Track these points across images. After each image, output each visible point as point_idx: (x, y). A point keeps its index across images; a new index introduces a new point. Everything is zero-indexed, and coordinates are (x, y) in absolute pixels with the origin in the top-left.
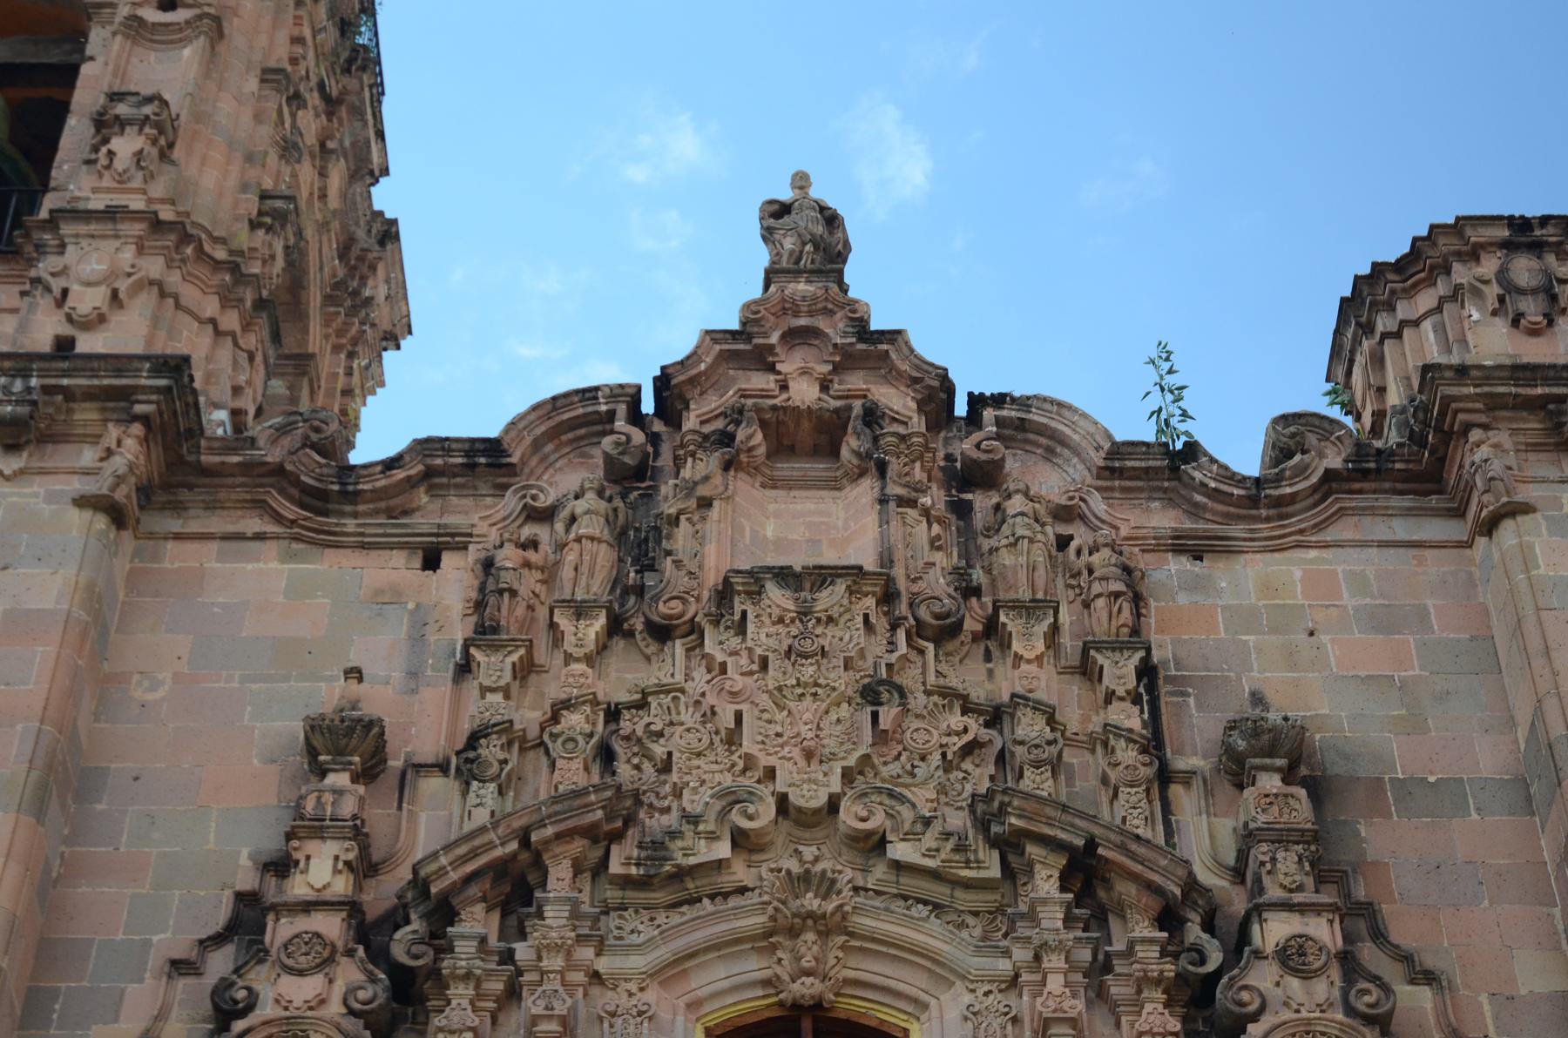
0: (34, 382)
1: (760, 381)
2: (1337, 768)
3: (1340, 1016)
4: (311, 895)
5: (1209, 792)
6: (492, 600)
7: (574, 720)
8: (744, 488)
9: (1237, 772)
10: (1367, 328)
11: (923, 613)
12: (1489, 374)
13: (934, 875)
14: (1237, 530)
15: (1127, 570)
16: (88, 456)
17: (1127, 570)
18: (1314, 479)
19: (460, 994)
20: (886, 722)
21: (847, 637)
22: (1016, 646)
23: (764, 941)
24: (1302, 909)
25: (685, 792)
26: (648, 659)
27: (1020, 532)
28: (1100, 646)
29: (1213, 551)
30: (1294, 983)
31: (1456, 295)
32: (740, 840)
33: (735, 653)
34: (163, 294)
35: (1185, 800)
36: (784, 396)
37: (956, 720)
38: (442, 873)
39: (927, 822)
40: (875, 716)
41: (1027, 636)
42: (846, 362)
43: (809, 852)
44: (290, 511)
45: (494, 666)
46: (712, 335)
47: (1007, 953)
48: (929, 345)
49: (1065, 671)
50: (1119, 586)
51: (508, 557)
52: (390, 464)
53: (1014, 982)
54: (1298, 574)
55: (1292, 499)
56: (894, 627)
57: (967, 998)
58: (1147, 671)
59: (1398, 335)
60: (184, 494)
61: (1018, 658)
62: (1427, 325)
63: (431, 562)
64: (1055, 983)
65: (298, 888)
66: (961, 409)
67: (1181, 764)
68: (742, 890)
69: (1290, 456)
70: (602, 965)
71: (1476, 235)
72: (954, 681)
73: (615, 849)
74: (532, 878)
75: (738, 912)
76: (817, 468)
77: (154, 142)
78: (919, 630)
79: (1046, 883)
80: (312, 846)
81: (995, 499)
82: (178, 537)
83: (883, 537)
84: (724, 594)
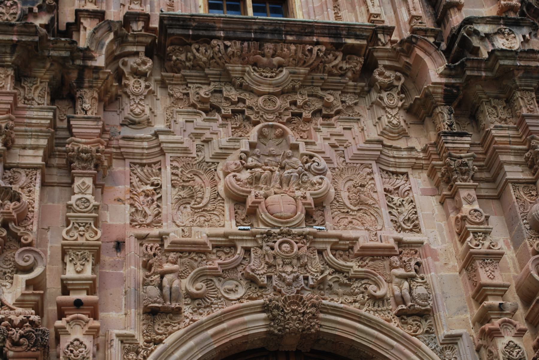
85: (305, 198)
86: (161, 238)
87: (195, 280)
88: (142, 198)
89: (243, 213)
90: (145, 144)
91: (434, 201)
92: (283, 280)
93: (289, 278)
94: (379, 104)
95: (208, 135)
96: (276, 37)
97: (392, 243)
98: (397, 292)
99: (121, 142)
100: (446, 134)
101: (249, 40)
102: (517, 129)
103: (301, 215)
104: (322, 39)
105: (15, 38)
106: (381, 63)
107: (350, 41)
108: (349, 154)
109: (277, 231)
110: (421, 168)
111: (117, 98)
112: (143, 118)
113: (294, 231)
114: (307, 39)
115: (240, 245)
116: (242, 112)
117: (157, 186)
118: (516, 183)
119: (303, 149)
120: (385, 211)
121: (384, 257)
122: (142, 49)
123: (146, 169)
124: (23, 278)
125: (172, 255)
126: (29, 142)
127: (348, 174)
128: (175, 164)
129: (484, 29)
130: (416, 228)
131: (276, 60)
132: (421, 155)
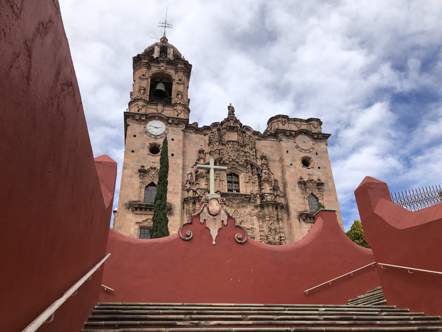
1: (228, 123)
2: (268, 158)
6: (211, 140)
7: (217, 151)
8: (227, 132)
10: (271, 121)
13: (241, 164)
15: (254, 141)
16: (181, 126)
20: (239, 153)
21: (236, 146)
23: (230, 168)
24: (266, 170)
28: (253, 148)
29: (260, 140)
32: (229, 161)
35: (258, 160)
37: (243, 153)
39: (242, 161)
42: (235, 122)
43: (233, 162)
44: (195, 131)
45: (211, 146)
46: (225, 119)
50: (254, 143)
51: (211, 136)
52: (202, 128)
53: (247, 173)
55: (266, 136)
56: (239, 145)
57: (244, 174)
58: (256, 150)
59: (274, 123)
60: (186, 128)
62: (276, 122)
63: (205, 136)
64: (250, 173)
66: (243, 126)
67: (258, 157)
69: (266, 133)
75: (229, 166)
76: (232, 130)
77: (182, 96)
79: (249, 166)
80: (201, 160)
81: (245, 135)
83: (238, 137)
84: (227, 142)
96: (237, 196)
97: (250, 228)
98: (250, 235)
100: (259, 212)
104: (244, 196)
108: (246, 213)
110: (256, 215)
114: (242, 196)
118: (267, 220)
119: (240, 213)
121: (249, 230)
127: (245, 217)
129: (266, 195)
131: (237, 199)
132: (256, 214)
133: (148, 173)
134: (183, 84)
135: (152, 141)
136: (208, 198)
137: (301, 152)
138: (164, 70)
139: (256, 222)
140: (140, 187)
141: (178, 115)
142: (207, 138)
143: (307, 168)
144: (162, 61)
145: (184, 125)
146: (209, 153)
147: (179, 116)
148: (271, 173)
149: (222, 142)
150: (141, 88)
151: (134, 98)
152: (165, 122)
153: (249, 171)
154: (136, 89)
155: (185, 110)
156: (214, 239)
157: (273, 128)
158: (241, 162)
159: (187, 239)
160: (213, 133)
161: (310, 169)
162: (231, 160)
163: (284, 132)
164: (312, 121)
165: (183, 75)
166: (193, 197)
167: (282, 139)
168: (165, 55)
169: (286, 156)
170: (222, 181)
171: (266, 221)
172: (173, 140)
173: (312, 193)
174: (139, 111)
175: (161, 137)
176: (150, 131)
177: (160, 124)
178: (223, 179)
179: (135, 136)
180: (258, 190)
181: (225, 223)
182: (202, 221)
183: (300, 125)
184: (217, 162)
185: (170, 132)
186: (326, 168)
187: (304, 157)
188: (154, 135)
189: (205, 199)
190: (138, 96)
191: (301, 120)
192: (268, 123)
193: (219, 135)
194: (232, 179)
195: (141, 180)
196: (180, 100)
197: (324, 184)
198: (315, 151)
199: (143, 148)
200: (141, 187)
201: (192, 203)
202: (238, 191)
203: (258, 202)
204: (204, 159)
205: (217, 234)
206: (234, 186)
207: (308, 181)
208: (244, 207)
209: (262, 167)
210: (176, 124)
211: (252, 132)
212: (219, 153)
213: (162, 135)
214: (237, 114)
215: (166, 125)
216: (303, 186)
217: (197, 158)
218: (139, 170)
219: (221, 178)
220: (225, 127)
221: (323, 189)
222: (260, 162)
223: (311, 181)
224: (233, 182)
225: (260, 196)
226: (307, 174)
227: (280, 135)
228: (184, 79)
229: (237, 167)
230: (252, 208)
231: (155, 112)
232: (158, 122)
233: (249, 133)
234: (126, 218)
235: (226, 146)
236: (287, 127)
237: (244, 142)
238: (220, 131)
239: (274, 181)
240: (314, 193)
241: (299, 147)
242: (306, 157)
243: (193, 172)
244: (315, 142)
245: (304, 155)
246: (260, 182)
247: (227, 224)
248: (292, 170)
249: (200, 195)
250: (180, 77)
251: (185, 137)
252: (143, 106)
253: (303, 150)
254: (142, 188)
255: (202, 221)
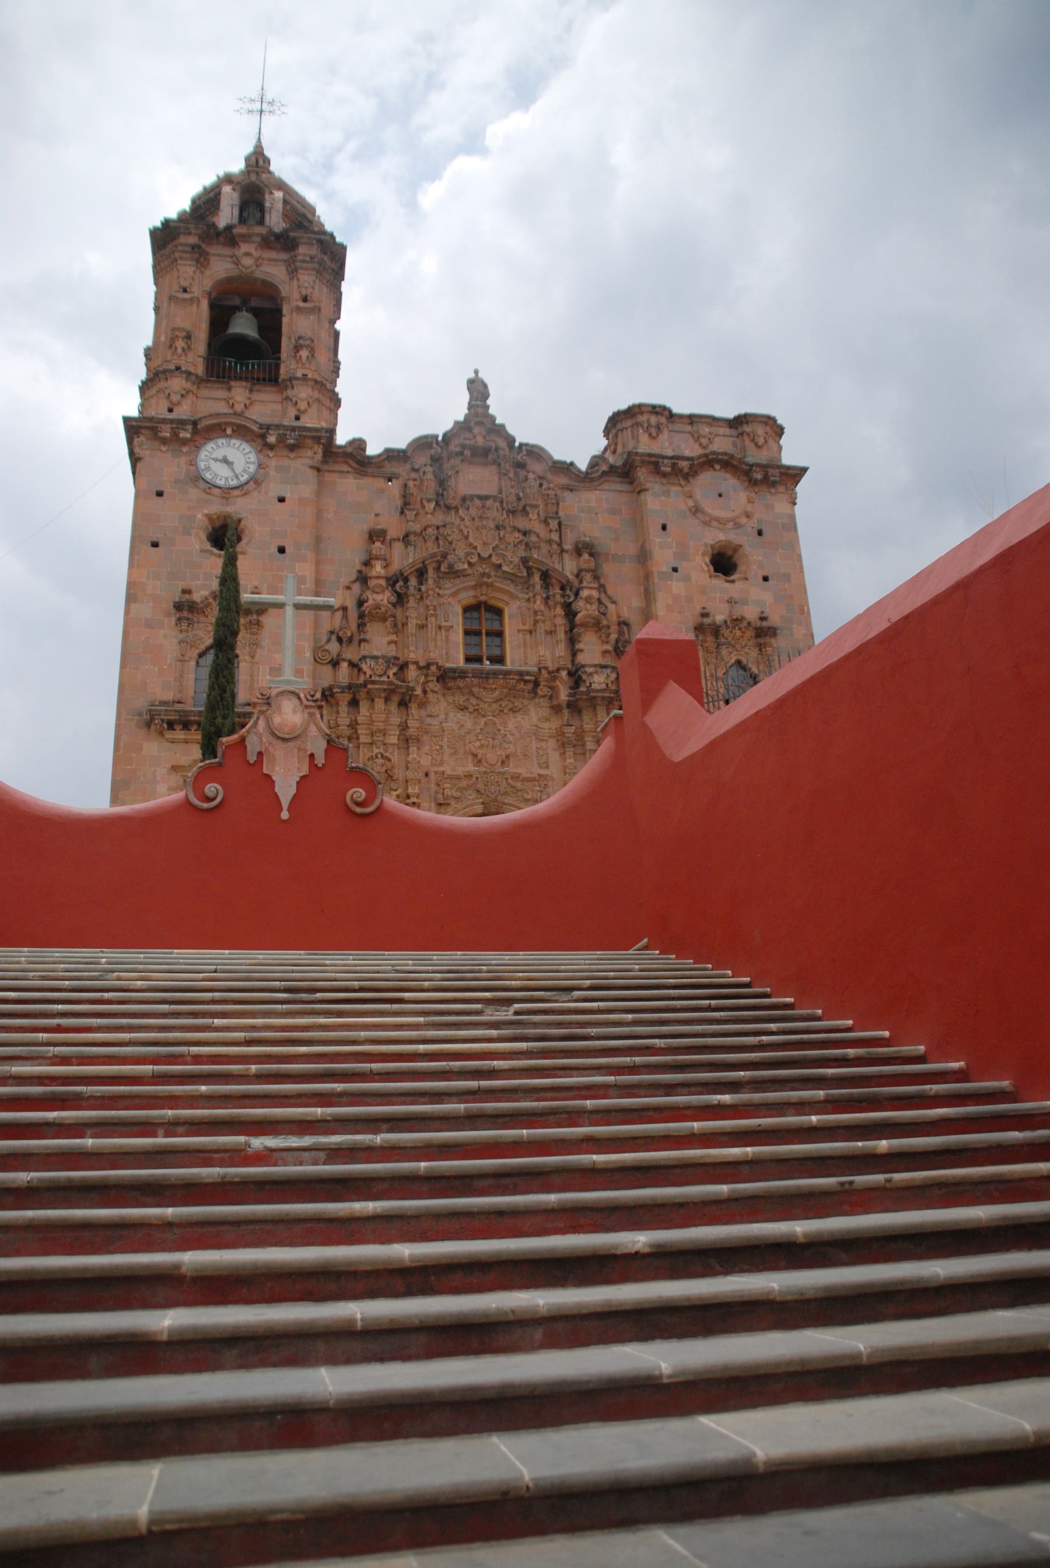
0: (296, 433)
1: (468, 435)
3: (597, 613)
4: (377, 575)
5: (571, 554)
7: (430, 530)
9: (578, 551)
10: (615, 426)
11: (509, 506)
12: (643, 455)
13: (513, 574)
14: (581, 485)
16: (309, 453)
17: (556, 495)
18: (600, 473)
19: (411, 599)
20: (501, 536)
21: (493, 514)
22: (531, 516)
23: (475, 587)
25: (456, 551)
26: (444, 513)
27: (532, 484)
29: (576, 490)
30: (588, 606)
31: (637, 424)
32: (470, 564)
33: (466, 515)
34: (319, 402)
35: (566, 556)
36: (474, 440)
37: (517, 535)
38: (407, 571)
40: (499, 534)
41: (533, 513)
43: (484, 566)
46: (456, 423)
47: (527, 593)
48: (511, 430)
49: (540, 521)
50: (554, 501)
51: (411, 483)
53: (529, 600)
54: (594, 497)
57: (518, 603)
58: (560, 524)
59: (622, 430)
61: (530, 520)
62: (629, 429)
64: (538, 602)
65: (374, 573)
66: (517, 444)
68: (469, 575)
70: (441, 592)
71: (643, 409)
72: (516, 525)
73: (442, 565)
74: (424, 571)
77: (310, 352)
78: (509, 511)
79: (536, 578)
81: (525, 473)
82: (329, 471)
84: (464, 499)
85: (501, 755)
86: (443, 773)
87: (456, 790)
88: (435, 752)
89: (476, 761)
90: (437, 727)
91: (557, 754)
92: (490, 792)
93: (493, 791)
94: (538, 705)
95: (463, 723)
97: (535, 775)
98: (535, 797)
99: (427, 727)
101: (482, 678)
102: (595, 724)
103: (499, 763)
105: (385, 687)
106: (542, 683)
107: (527, 678)
109: (489, 771)
110: (554, 737)
111: (425, 703)
112: (435, 714)
113: (496, 771)
114: (508, 677)
115: (474, 776)
116: (478, 710)
117: (442, 747)
119: (502, 732)
120: (535, 759)
121: (531, 781)
122: (435, 679)
123: (437, 738)
124: (395, 793)
125: (448, 780)
126: (392, 733)
128: (449, 736)
129: (589, 670)
130: (547, 767)
131: (494, 686)
132: (554, 731)
133: (204, 612)
134: (317, 310)
135: (216, 508)
136: (272, 690)
137: (708, 528)
138: (251, 267)
139: (554, 756)
140: (182, 658)
141: (297, 418)
142: (394, 488)
143: (727, 581)
144: (246, 238)
145: (320, 451)
146: (403, 539)
147: (301, 420)
148: (610, 598)
149: (447, 499)
150: (177, 333)
151: (154, 368)
152: (255, 441)
153: (534, 596)
154: (163, 338)
155: (323, 399)
156: (285, 803)
157: (619, 450)
158: (507, 565)
159: (206, 805)
160: (414, 470)
161: (737, 583)
162: (474, 559)
163: (654, 463)
164: (750, 424)
165: (314, 282)
166: (350, 684)
167: (648, 485)
168: (258, 215)
169: (658, 540)
170: (446, 631)
171: (588, 752)
172: (282, 500)
173: (739, 662)
174: (170, 410)
175: (244, 492)
176: (208, 476)
177: (241, 449)
178: (449, 624)
179: (160, 494)
180: (562, 654)
181: (320, 761)
182: (252, 758)
183: (709, 439)
184: (428, 567)
185: (271, 473)
186: (787, 577)
187: (718, 542)
188: (220, 488)
189: (262, 694)
190: (168, 361)
191: (712, 420)
192: (607, 432)
193: (435, 477)
194: (480, 624)
195: (184, 635)
196: (303, 364)
197: (776, 630)
198: (753, 524)
199: (187, 532)
200: (183, 655)
201: (346, 703)
202: (500, 660)
203: (564, 695)
204: (385, 560)
205: (293, 790)
206: (486, 646)
207: (726, 622)
208: (515, 711)
209: (580, 578)
210: (292, 448)
211: (547, 464)
212: (437, 539)
213: (245, 488)
214: (496, 407)
215: (261, 451)
216: (710, 638)
217: (362, 557)
218: (175, 603)
219: (443, 619)
220: (458, 449)
221: (775, 645)
222: (575, 563)
223: (737, 621)
224: (484, 631)
225: (570, 674)
226: (726, 599)
227: (642, 474)
228: (321, 293)
229: (495, 581)
230: (545, 712)
231: (226, 411)
232: (232, 445)
233: (538, 468)
234: (143, 753)
235: (461, 512)
236: (667, 445)
237: (519, 499)
238: (441, 465)
239: (619, 624)
240: (744, 662)
241: (703, 512)
242: (728, 544)
243: (351, 604)
244: (756, 493)
245: (716, 536)
246: (572, 626)
247: (323, 765)
248: (677, 586)
249: (373, 679)
250: (306, 288)
251: (321, 488)
252: (183, 392)
253: (718, 520)
254: (187, 659)
255: (252, 758)
